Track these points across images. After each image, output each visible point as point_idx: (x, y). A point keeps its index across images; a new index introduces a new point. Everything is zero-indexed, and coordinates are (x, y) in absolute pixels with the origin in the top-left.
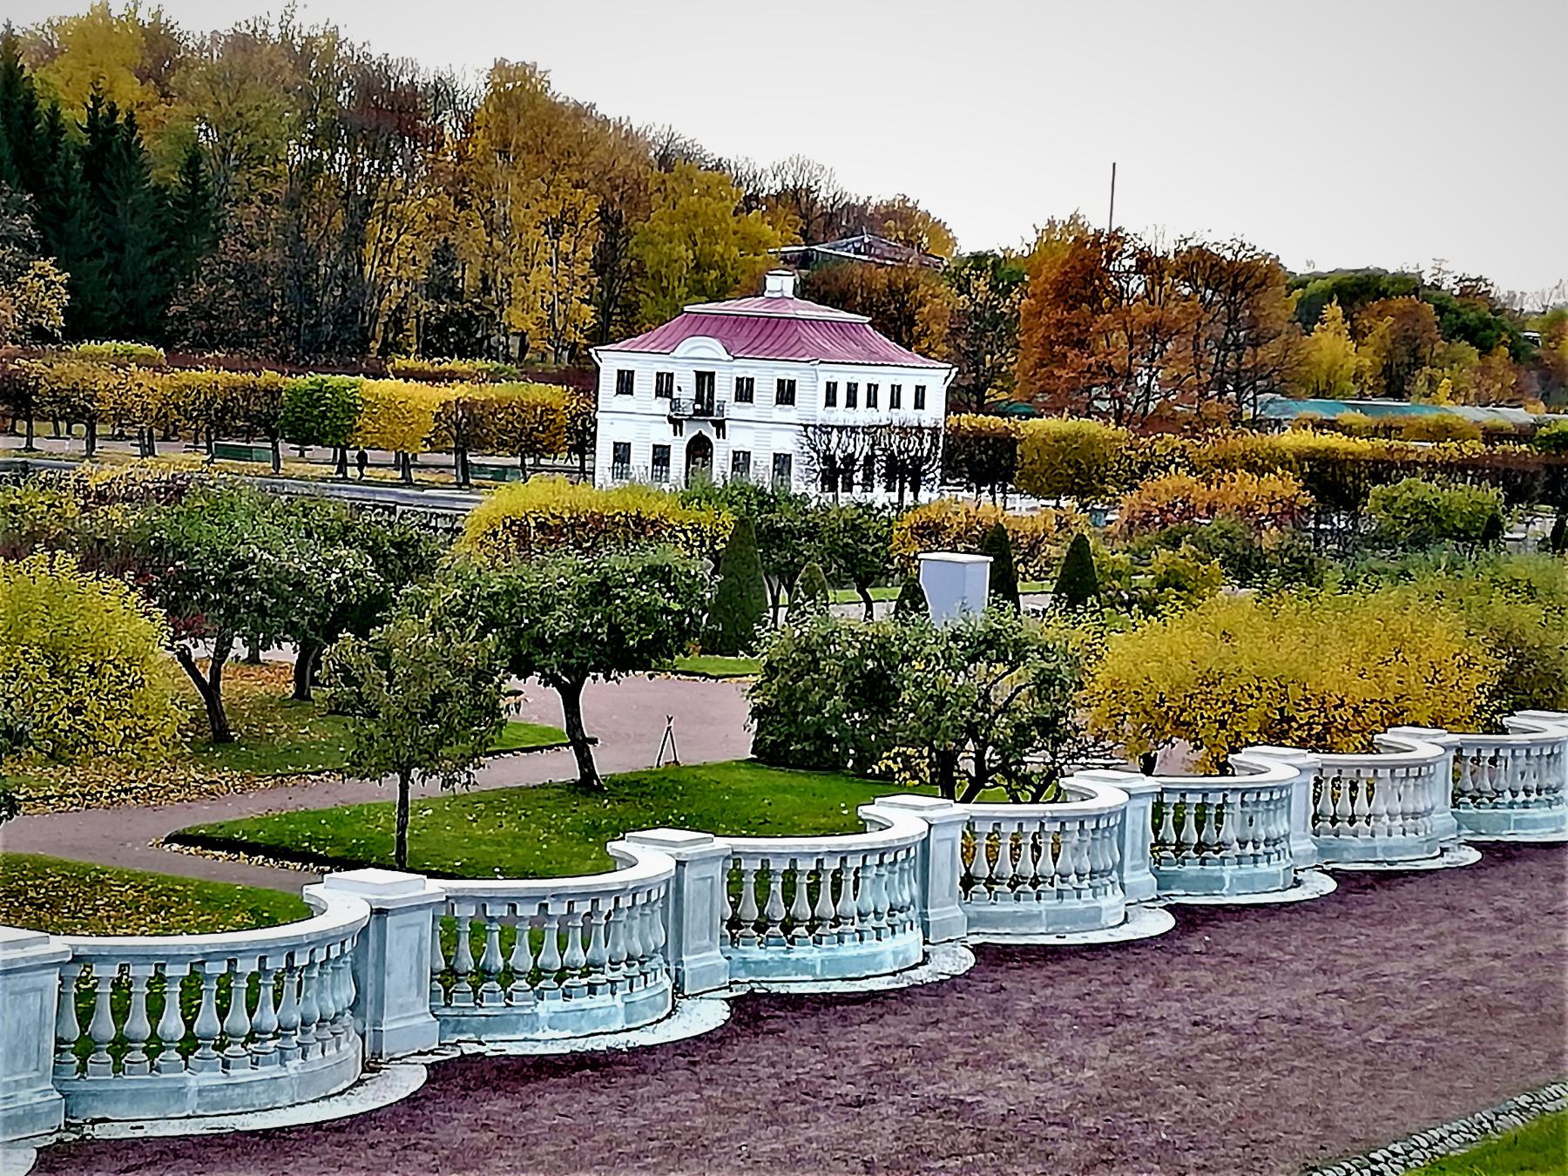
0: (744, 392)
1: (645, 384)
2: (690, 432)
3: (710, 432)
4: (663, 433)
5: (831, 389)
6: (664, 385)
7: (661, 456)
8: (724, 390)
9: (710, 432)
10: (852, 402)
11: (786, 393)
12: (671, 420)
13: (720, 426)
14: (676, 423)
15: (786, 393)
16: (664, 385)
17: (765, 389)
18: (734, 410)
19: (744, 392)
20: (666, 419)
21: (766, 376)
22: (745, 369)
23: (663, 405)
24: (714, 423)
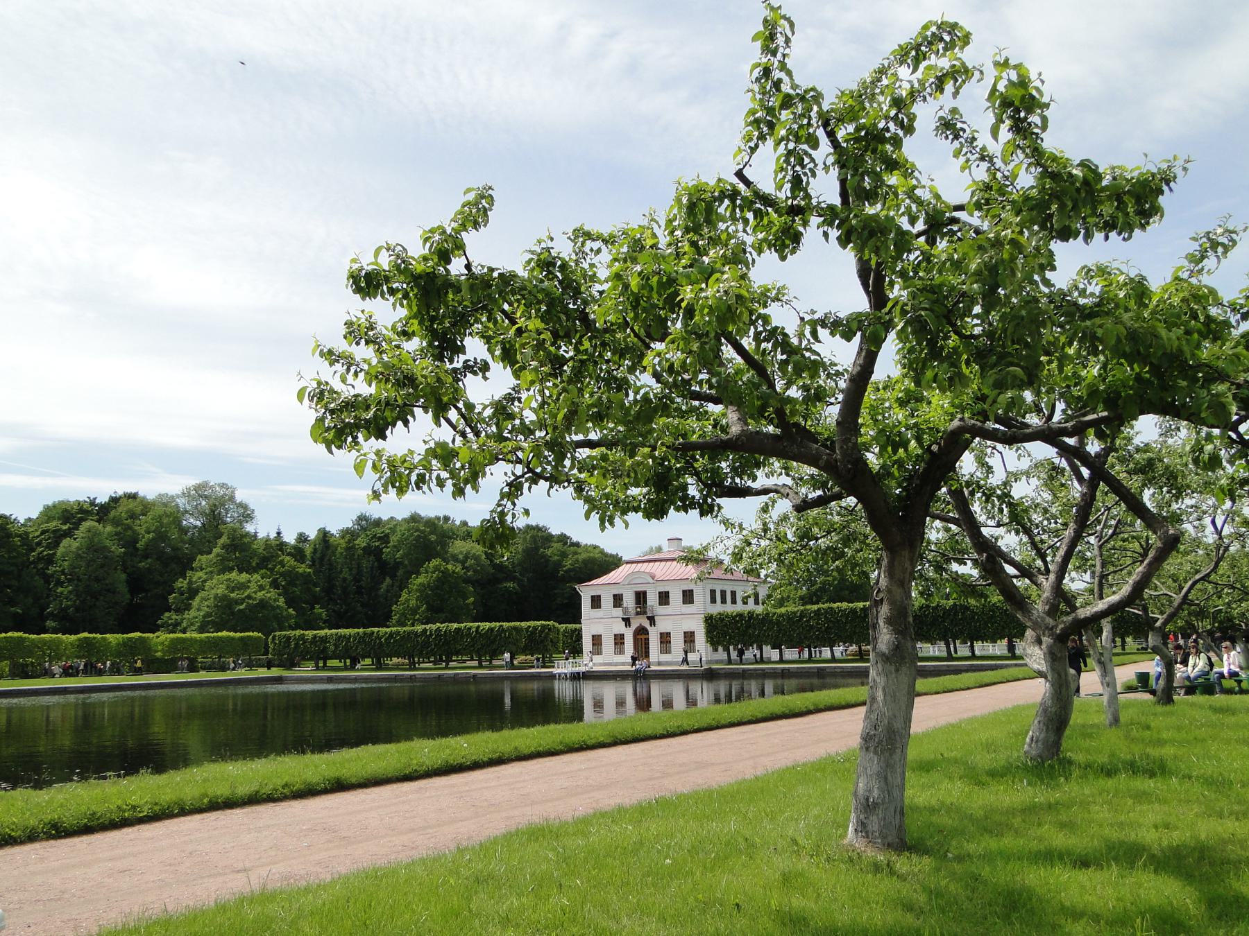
0: (664, 598)
1: (607, 601)
2: (635, 625)
3: (646, 624)
4: (620, 628)
5: (713, 592)
6: (618, 600)
7: (619, 639)
8: (652, 599)
10: (724, 601)
11: (688, 597)
12: (623, 619)
13: (652, 620)
14: (627, 621)
15: (688, 597)
16: (618, 600)
17: (676, 597)
23: (618, 612)
24: (649, 618)
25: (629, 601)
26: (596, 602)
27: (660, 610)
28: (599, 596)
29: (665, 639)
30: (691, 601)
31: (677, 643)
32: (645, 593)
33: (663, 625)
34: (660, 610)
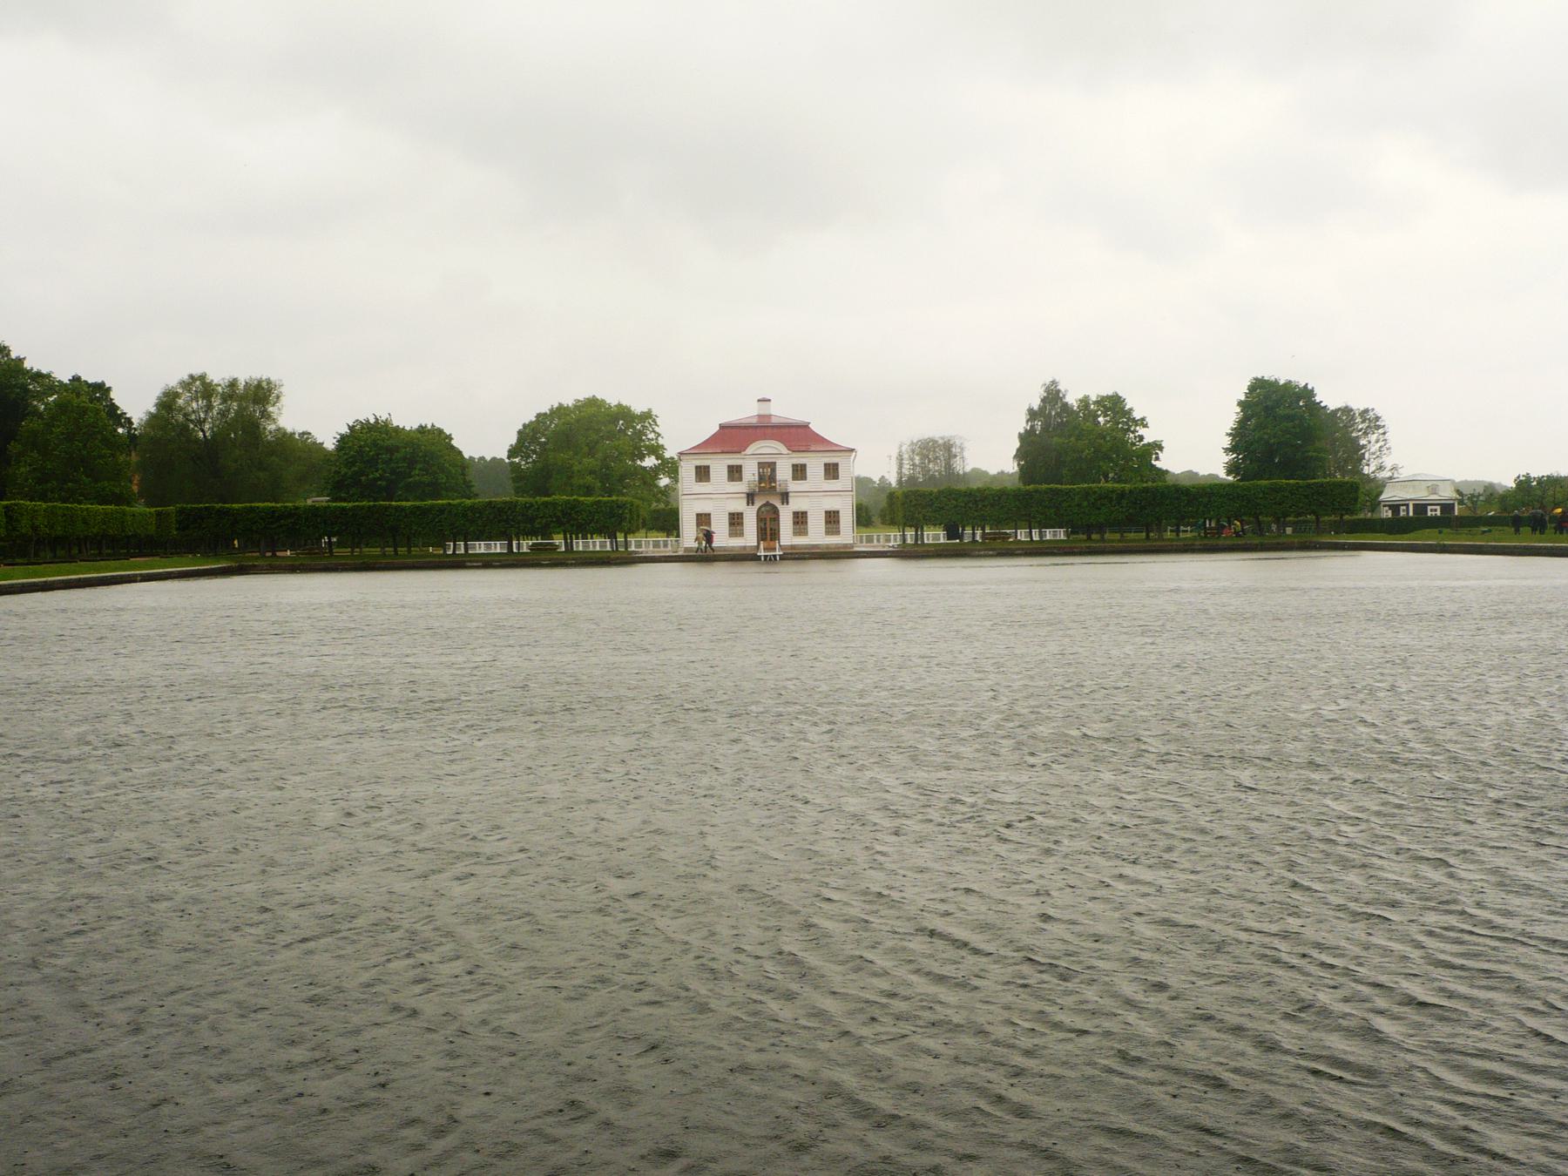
0: (799, 472)
2: (758, 504)
4: (739, 505)
6: (735, 473)
7: (736, 520)
8: (784, 473)
9: (777, 503)
11: (832, 471)
13: (785, 497)
14: (750, 498)
16: (735, 473)
18: (793, 486)
19: (799, 472)
20: (745, 495)
21: (815, 464)
22: (799, 459)
25: (751, 472)
26: (703, 473)
28: (707, 468)
29: (800, 519)
30: (836, 477)
31: (816, 525)
32: (772, 466)
33: (796, 504)
34: (793, 486)
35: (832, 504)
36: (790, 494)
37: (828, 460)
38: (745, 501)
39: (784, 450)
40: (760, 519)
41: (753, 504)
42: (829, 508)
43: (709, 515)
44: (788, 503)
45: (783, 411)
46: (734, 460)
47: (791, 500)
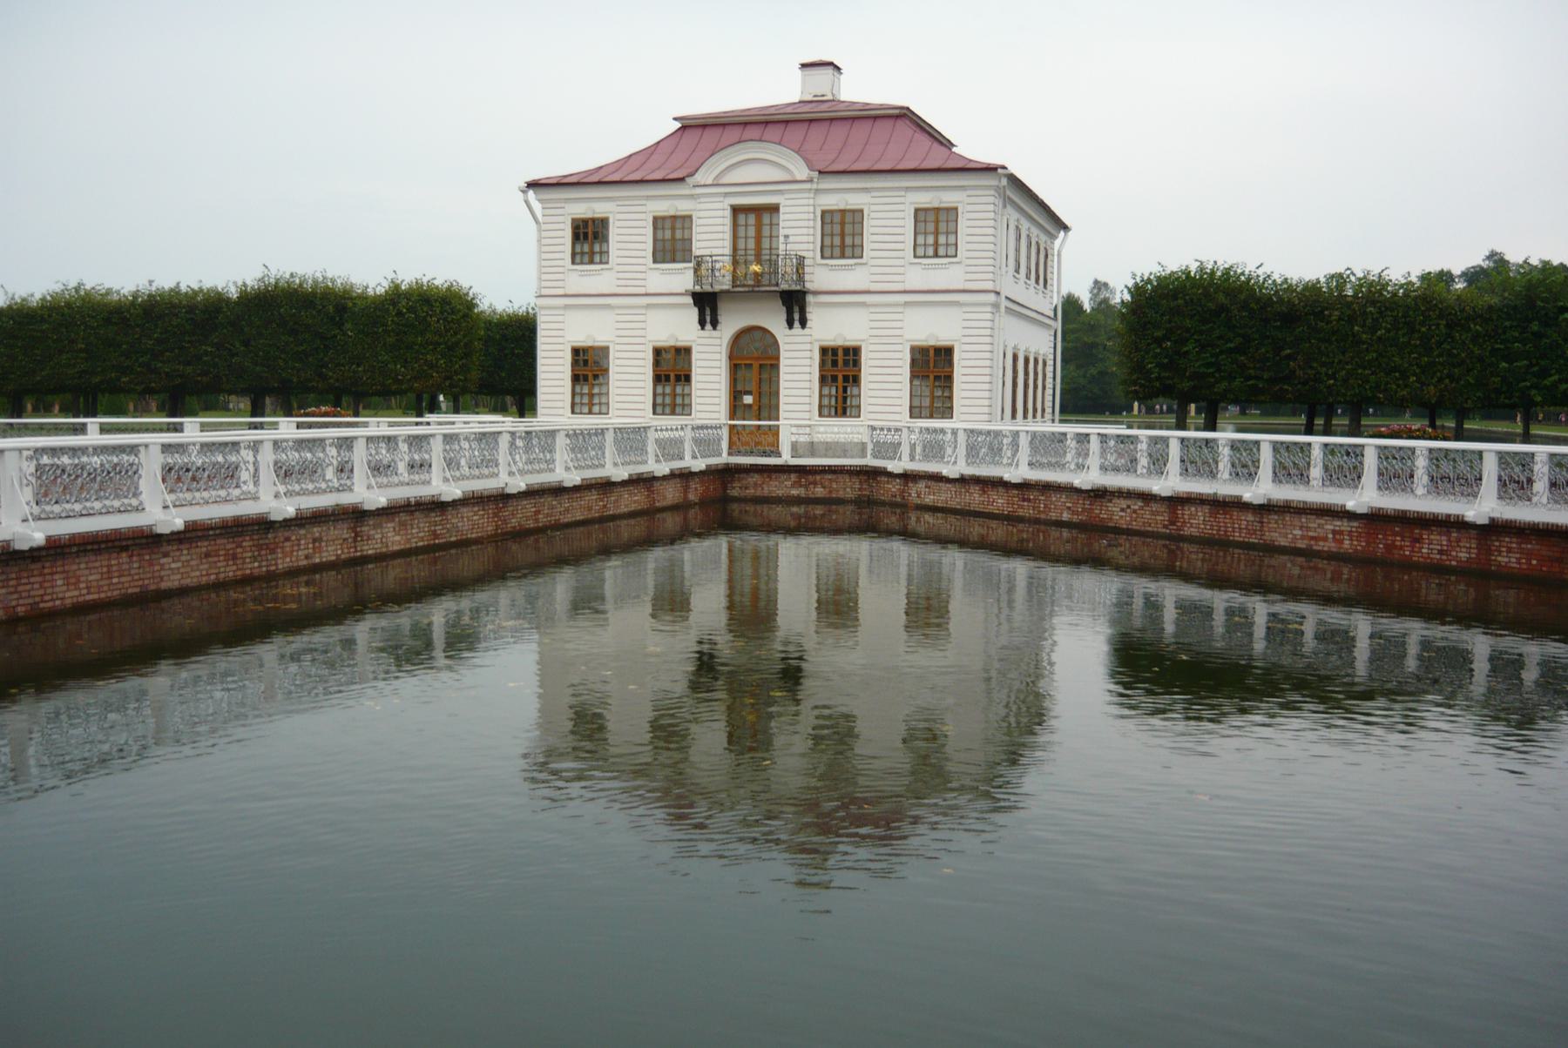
3: (773, 320)
4: (681, 326)
13: (795, 304)
14: (707, 305)
20: (690, 300)
22: (842, 196)
23: (680, 278)
27: (821, 276)
35: (932, 328)
36: (810, 299)
37: (926, 199)
38: (694, 313)
39: (801, 171)
40: (737, 365)
41: (715, 324)
42: (582, 340)
43: (604, 351)
44: (803, 323)
45: (835, 63)
46: (666, 203)
47: (813, 315)
